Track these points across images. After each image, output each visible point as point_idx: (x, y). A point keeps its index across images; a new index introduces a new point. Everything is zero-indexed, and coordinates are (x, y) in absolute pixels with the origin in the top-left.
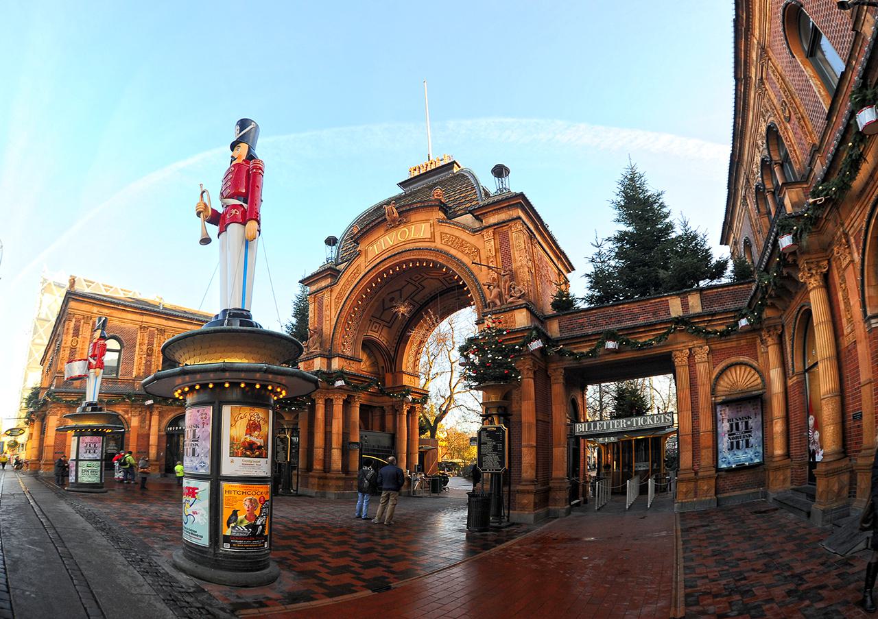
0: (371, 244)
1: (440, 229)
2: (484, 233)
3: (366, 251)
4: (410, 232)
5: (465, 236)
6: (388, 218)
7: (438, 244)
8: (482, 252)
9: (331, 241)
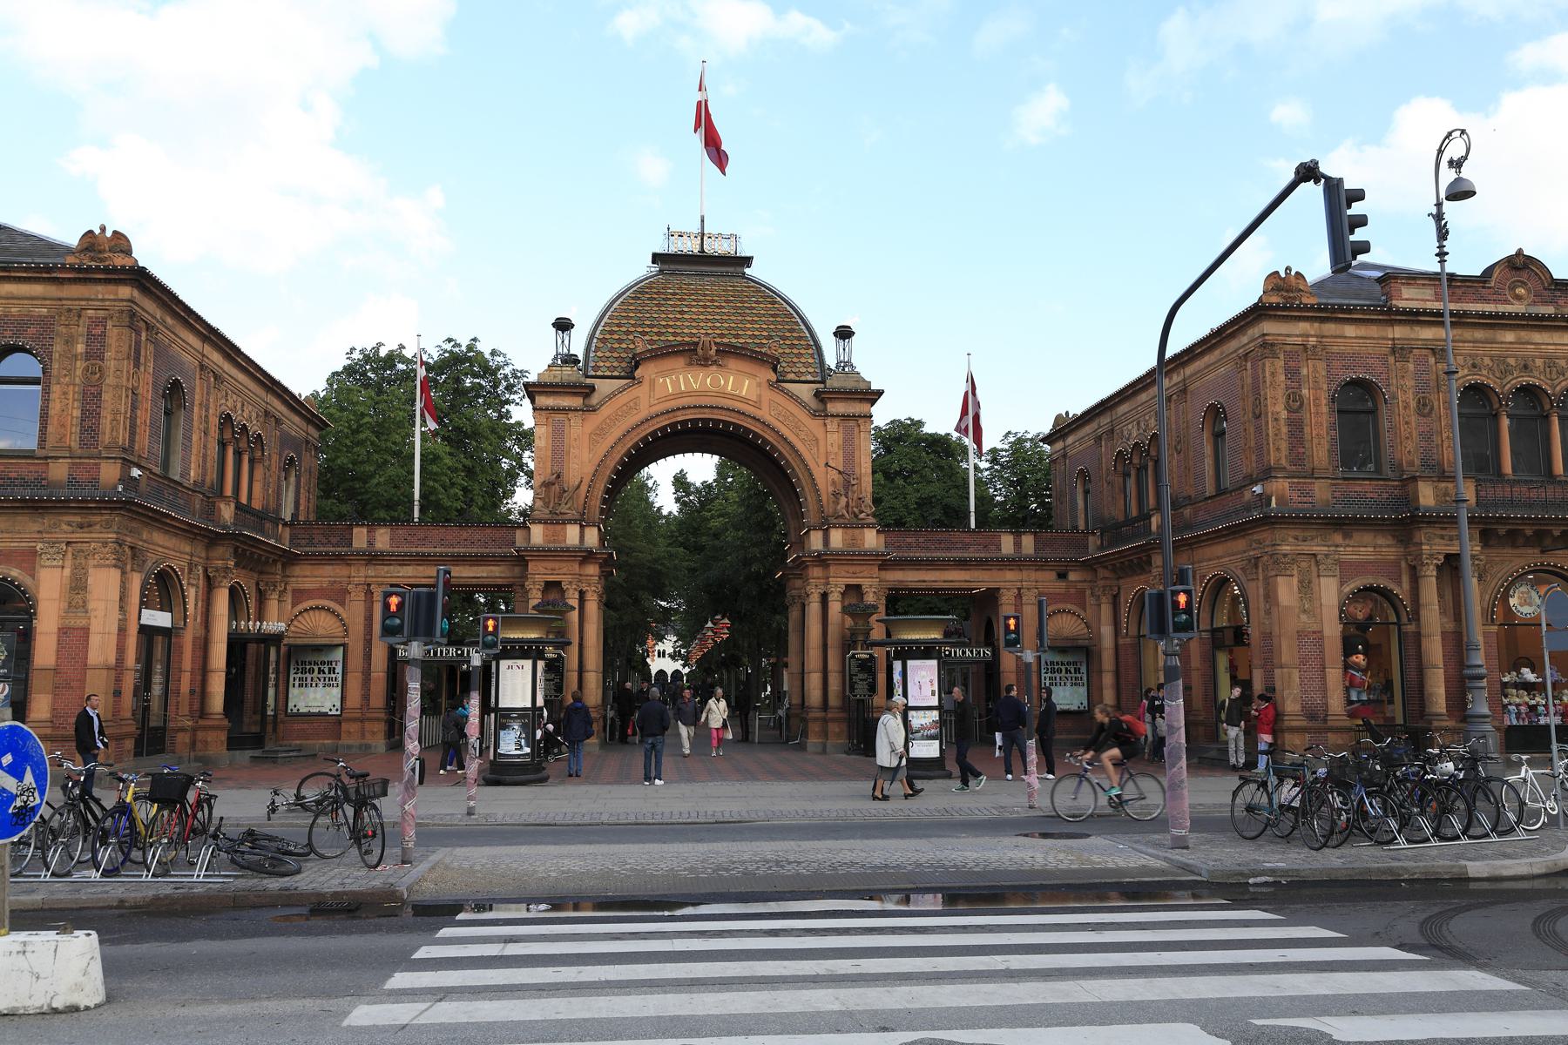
0: (664, 374)
1: (768, 394)
2: (828, 421)
3: (652, 383)
4: (726, 382)
5: (802, 415)
6: (700, 352)
7: (765, 414)
8: (822, 443)
9: (563, 325)
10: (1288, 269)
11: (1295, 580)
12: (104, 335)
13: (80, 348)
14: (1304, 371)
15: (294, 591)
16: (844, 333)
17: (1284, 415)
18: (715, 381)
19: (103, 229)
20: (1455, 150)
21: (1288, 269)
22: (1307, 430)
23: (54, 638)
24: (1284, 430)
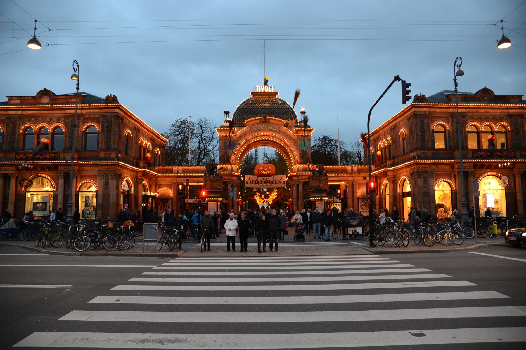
9: (227, 113)
10: (420, 94)
11: (422, 179)
12: (111, 121)
13: (106, 125)
14: (425, 122)
15: (159, 185)
16: (303, 113)
17: (419, 134)
18: (267, 127)
19: (111, 95)
20: (459, 63)
21: (420, 94)
22: (426, 138)
23: (102, 197)
24: (420, 138)
